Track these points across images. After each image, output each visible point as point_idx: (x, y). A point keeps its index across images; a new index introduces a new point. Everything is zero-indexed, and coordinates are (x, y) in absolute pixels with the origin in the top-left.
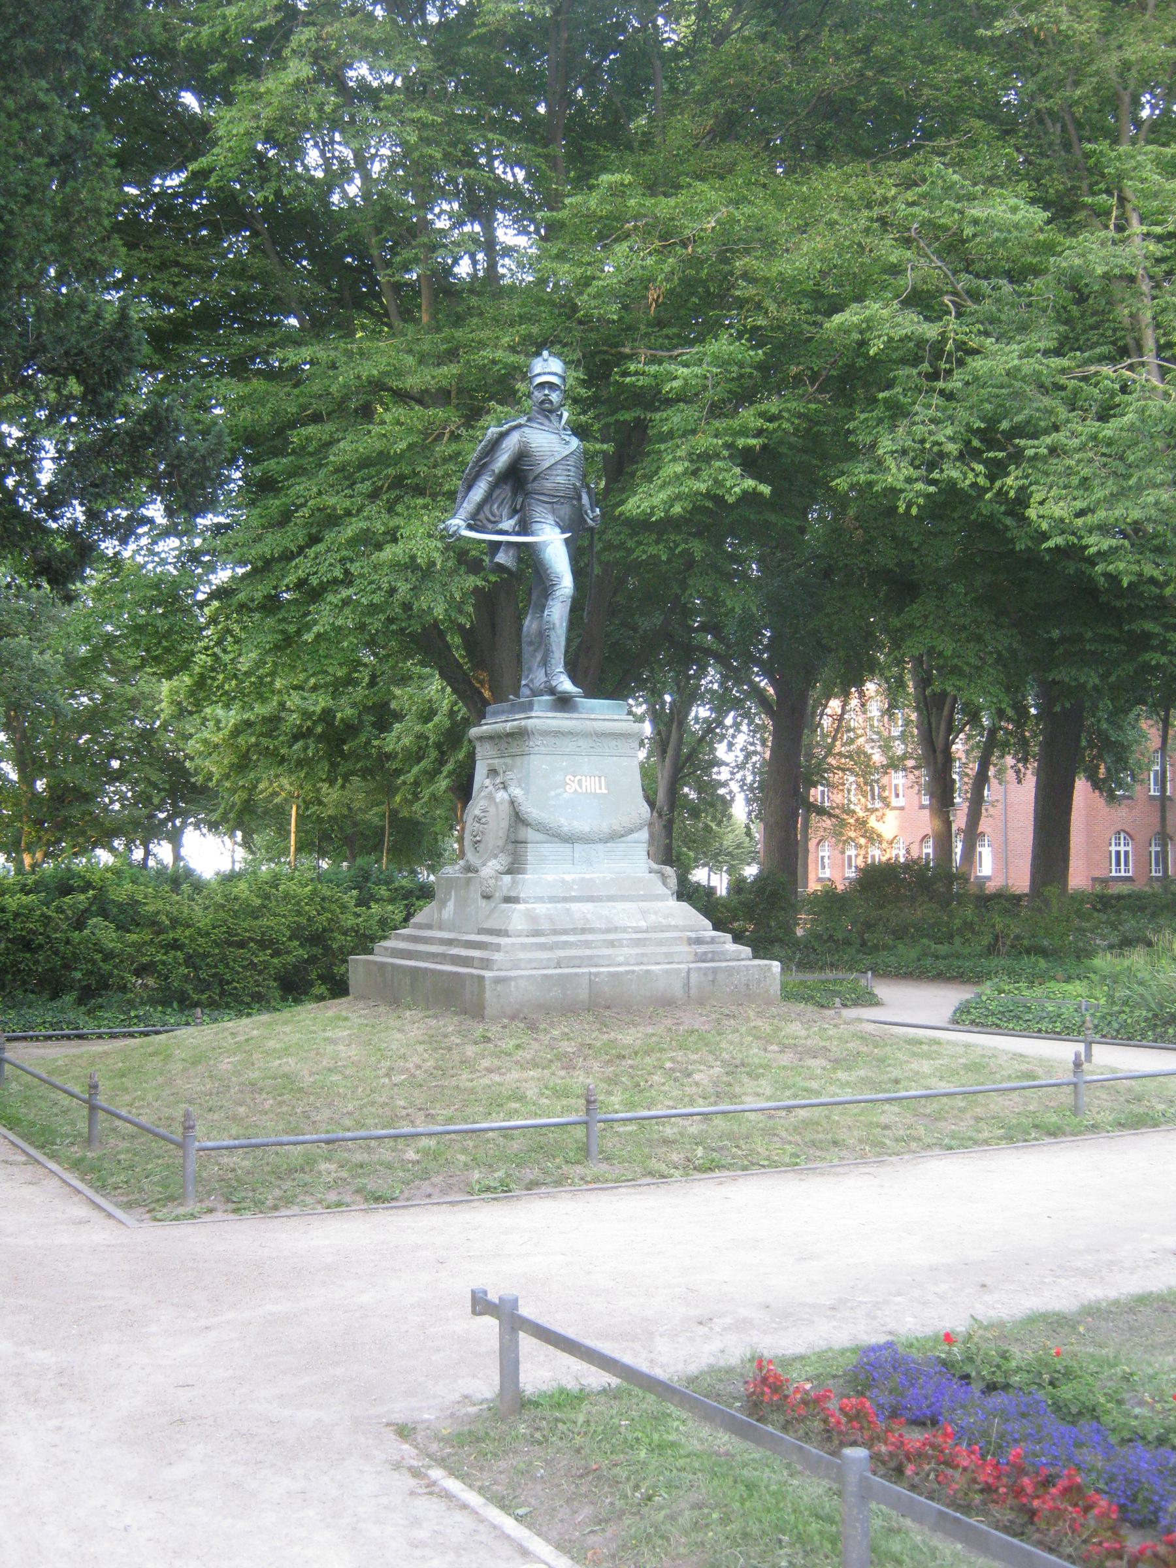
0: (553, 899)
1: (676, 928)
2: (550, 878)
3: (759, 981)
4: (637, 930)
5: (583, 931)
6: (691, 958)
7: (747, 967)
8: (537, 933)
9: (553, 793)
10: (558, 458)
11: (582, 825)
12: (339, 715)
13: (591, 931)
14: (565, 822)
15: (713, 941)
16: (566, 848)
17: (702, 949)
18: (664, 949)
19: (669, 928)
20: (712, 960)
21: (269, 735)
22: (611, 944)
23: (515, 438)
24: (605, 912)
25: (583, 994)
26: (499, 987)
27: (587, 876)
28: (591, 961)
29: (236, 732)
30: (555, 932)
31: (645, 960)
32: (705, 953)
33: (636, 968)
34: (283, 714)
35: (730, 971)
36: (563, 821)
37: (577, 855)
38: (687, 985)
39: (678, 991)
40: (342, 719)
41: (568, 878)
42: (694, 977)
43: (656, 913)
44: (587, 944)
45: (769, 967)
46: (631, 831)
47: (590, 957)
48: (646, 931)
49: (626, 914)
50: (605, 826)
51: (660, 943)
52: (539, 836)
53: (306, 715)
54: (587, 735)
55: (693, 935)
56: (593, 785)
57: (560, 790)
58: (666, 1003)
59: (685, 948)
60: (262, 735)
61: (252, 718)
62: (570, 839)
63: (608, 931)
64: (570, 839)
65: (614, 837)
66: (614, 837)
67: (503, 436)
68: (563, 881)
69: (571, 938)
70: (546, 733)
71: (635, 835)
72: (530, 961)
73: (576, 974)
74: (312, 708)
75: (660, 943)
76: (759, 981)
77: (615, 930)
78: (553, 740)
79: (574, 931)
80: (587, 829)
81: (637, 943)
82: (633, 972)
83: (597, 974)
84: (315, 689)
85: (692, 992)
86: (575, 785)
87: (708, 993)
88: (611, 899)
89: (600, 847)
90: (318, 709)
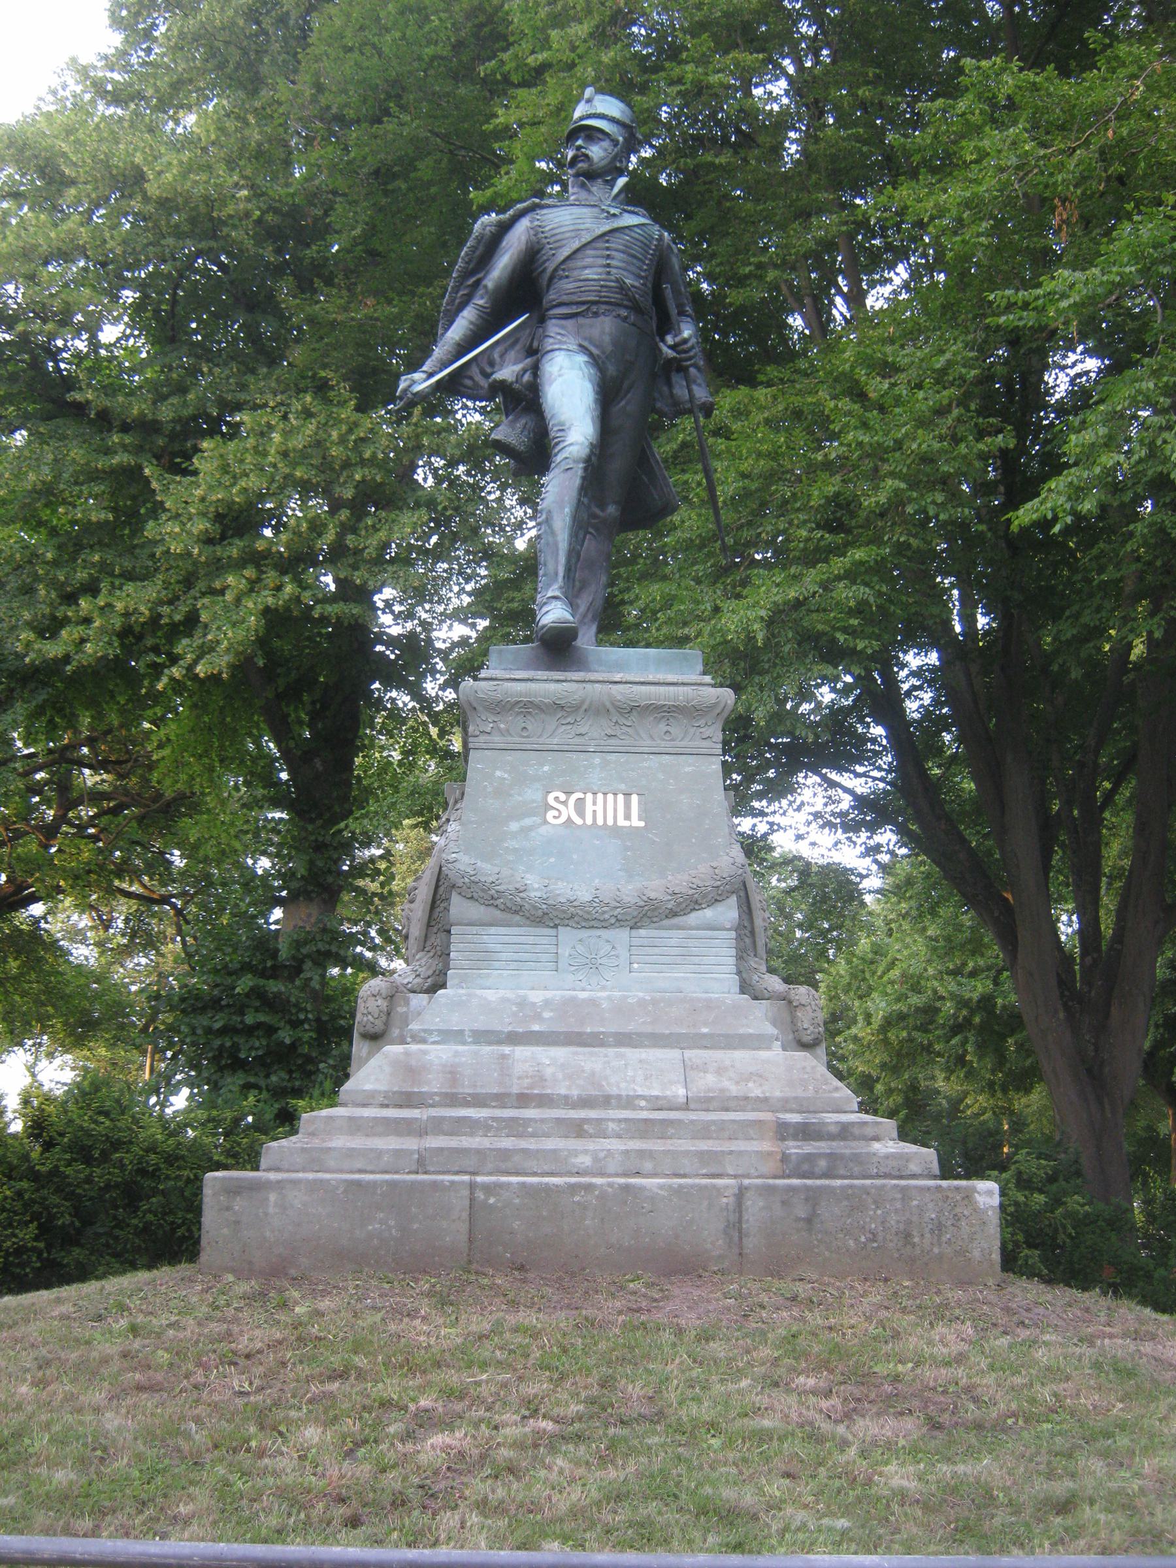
1: (763, 1103)
2: (491, 995)
3: (939, 1227)
4: (657, 1104)
5: (524, 1100)
6: (768, 1167)
7: (903, 1189)
8: (407, 1100)
9: (514, 826)
10: (587, 238)
11: (578, 890)
12: (999, 1001)
13: (544, 1101)
14: (534, 883)
15: (845, 1132)
16: (540, 937)
19: (744, 1102)
21: (923, 1028)
22: (578, 1129)
23: (524, 224)
25: (454, 1231)
26: (238, 1204)
28: (504, 1160)
29: (888, 1023)
30: (452, 1100)
31: (648, 1166)
32: (809, 1158)
34: (938, 1004)
35: (855, 1201)
37: (565, 951)
38: (735, 1227)
40: (1004, 1007)
41: (537, 997)
42: (754, 1207)
43: (720, 1071)
45: (968, 1196)
46: (693, 903)
47: (505, 1154)
48: (686, 1107)
50: (630, 891)
51: (704, 1131)
53: (963, 1003)
55: (794, 1118)
57: (528, 822)
58: (679, 1265)
59: (766, 1146)
60: (916, 1028)
61: (905, 1009)
62: (548, 917)
63: (585, 1102)
64: (548, 917)
65: (647, 915)
66: (647, 915)
67: (504, 228)
68: (522, 1003)
70: (500, 707)
71: (708, 914)
72: (351, 1153)
74: (967, 995)
75: (704, 1131)
76: (939, 1227)
77: (606, 1101)
78: (520, 722)
79: (501, 1099)
80: (584, 895)
81: (644, 1129)
82: (589, 1187)
83: (488, 1189)
84: (973, 974)
85: (750, 1243)
86: (569, 811)
87: (784, 1247)
88: (625, 1040)
89: (622, 936)
90: (975, 996)
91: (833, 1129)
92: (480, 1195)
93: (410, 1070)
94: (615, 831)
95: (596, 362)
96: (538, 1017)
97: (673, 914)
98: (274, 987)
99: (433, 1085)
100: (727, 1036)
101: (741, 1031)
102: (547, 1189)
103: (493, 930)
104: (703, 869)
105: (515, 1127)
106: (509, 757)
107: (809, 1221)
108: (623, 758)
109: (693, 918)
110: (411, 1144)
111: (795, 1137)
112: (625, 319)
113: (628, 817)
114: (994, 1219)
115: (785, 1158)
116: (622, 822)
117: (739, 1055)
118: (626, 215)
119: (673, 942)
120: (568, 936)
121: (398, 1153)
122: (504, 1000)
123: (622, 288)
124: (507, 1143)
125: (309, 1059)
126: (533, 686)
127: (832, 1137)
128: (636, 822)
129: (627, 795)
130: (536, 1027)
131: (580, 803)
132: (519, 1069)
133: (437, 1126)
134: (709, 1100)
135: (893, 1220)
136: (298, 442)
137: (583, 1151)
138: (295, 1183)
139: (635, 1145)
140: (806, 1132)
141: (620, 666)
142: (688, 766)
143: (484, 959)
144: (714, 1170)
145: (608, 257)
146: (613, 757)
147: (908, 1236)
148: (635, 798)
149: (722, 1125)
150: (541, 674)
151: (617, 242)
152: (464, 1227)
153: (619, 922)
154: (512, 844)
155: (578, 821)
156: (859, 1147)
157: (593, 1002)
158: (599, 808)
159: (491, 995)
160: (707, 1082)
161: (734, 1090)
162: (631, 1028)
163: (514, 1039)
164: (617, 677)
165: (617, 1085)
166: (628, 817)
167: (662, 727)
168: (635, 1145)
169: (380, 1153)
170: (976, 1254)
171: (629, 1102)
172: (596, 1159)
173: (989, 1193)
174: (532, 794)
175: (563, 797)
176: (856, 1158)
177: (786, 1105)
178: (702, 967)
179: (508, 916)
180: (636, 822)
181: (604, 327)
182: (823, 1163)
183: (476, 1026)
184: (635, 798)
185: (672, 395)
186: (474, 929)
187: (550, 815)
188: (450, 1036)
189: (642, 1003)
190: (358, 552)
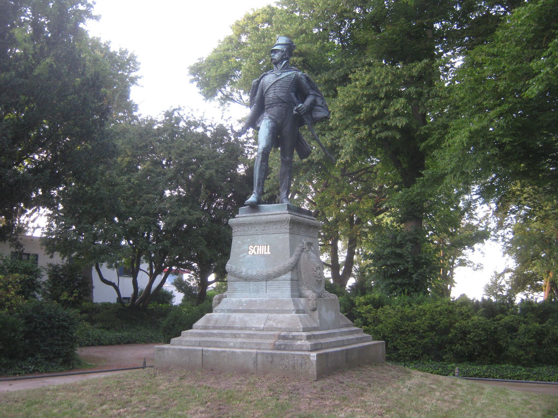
0: (230, 311)
3: (301, 365)
5: (229, 328)
7: (293, 355)
8: (205, 328)
9: (241, 256)
13: (233, 328)
14: (244, 270)
17: (281, 342)
18: (255, 341)
20: (284, 349)
22: (235, 336)
24: (247, 318)
25: (199, 361)
26: (160, 353)
27: (254, 299)
28: (216, 344)
30: (214, 328)
31: (245, 346)
32: (280, 345)
33: (238, 350)
35: (282, 357)
36: (244, 270)
38: (256, 363)
39: (251, 366)
41: (243, 300)
42: (260, 357)
44: (222, 335)
45: (308, 357)
48: (263, 330)
49: (257, 321)
51: (262, 337)
52: (232, 278)
55: (283, 333)
56: (263, 250)
57: (244, 254)
58: (243, 371)
62: (247, 279)
63: (241, 329)
64: (247, 279)
65: (268, 278)
66: (268, 278)
68: (240, 302)
69: (215, 331)
70: (239, 225)
71: (284, 276)
72: (187, 341)
73: (195, 350)
76: (301, 365)
77: (246, 328)
78: (243, 228)
79: (224, 328)
80: (254, 273)
81: (249, 336)
82: (225, 352)
83: (206, 351)
85: (259, 367)
86: (254, 251)
88: (259, 311)
89: (264, 283)
91: (291, 337)
92: (204, 353)
93: (209, 320)
94: (264, 255)
95: (273, 120)
96: (242, 305)
97: (276, 277)
98: (398, 251)
99: (211, 324)
100: (282, 310)
101: (286, 309)
102: (216, 352)
103: (236, 283)
104: (282, 265)
105: (222, 335)
106: (241, 237)
107: (272, 362)
108: (266, 235)
109: (281, 278)
110: (198, 339)
111: (282, 339)
112: (281, 106)
113: (267, 251)
114: (314, 363)
115: (274, 345)
116: (265, 253)
117: (281, 315)
118: (283, 74)
119: (276, 284)
120: (252, 284)
121: (195, 341)
122: (237, 301)
123: (279, 98)
126: (245, 219)
127: (290, 339)
128: (269, 253)
129: (267, 245)
130: (240, 308)
131: (256, 248)
132: (232, 319)
134: (267, 328)
135: (291, 362)
137: (231, 341)
138: (170, 349)
139: (245, 340)
140: (285, 338)
141: (268, 210)
142: (281, 236)
143: (235, 290)
144: (258, 347)
145: (275, 90)
146: (264, 235)
147: (294, 366)
148: (268, 246)
149: (266, 335)
150: (249, 215)
151: (278, 85)
152: (201, 360)
153: (262, 280)
154: (241, 260)
155: (255, 253)
157: (256, 301)
158: (260, 250)
159: (234, 299)
160: (271, 323)
161: (275, 325)
162: (261, 308)
163: (235, 311)
164: (266, 213)
165: (249, 325)
166: (267, 251)
167: (275, 226)
168: (245, 340)
169: (192, 341)
170: (310, 372)
171: (250, 329)
172: (234, 344)
173: (314, 356)
174: (245, 247)
175: (252, 247)
176: (291, 345)
177: (285, 330)
178: (282, 291)
179: (238, 279)
180: (269, 253)
181: (275, 110)
182: (283, 346)
183: (228, 308)
184: (268, 246)
185: (312, 117)
186: (233, 283)
187: (250, 252)
188: (222, 311)
189: (266, 301)
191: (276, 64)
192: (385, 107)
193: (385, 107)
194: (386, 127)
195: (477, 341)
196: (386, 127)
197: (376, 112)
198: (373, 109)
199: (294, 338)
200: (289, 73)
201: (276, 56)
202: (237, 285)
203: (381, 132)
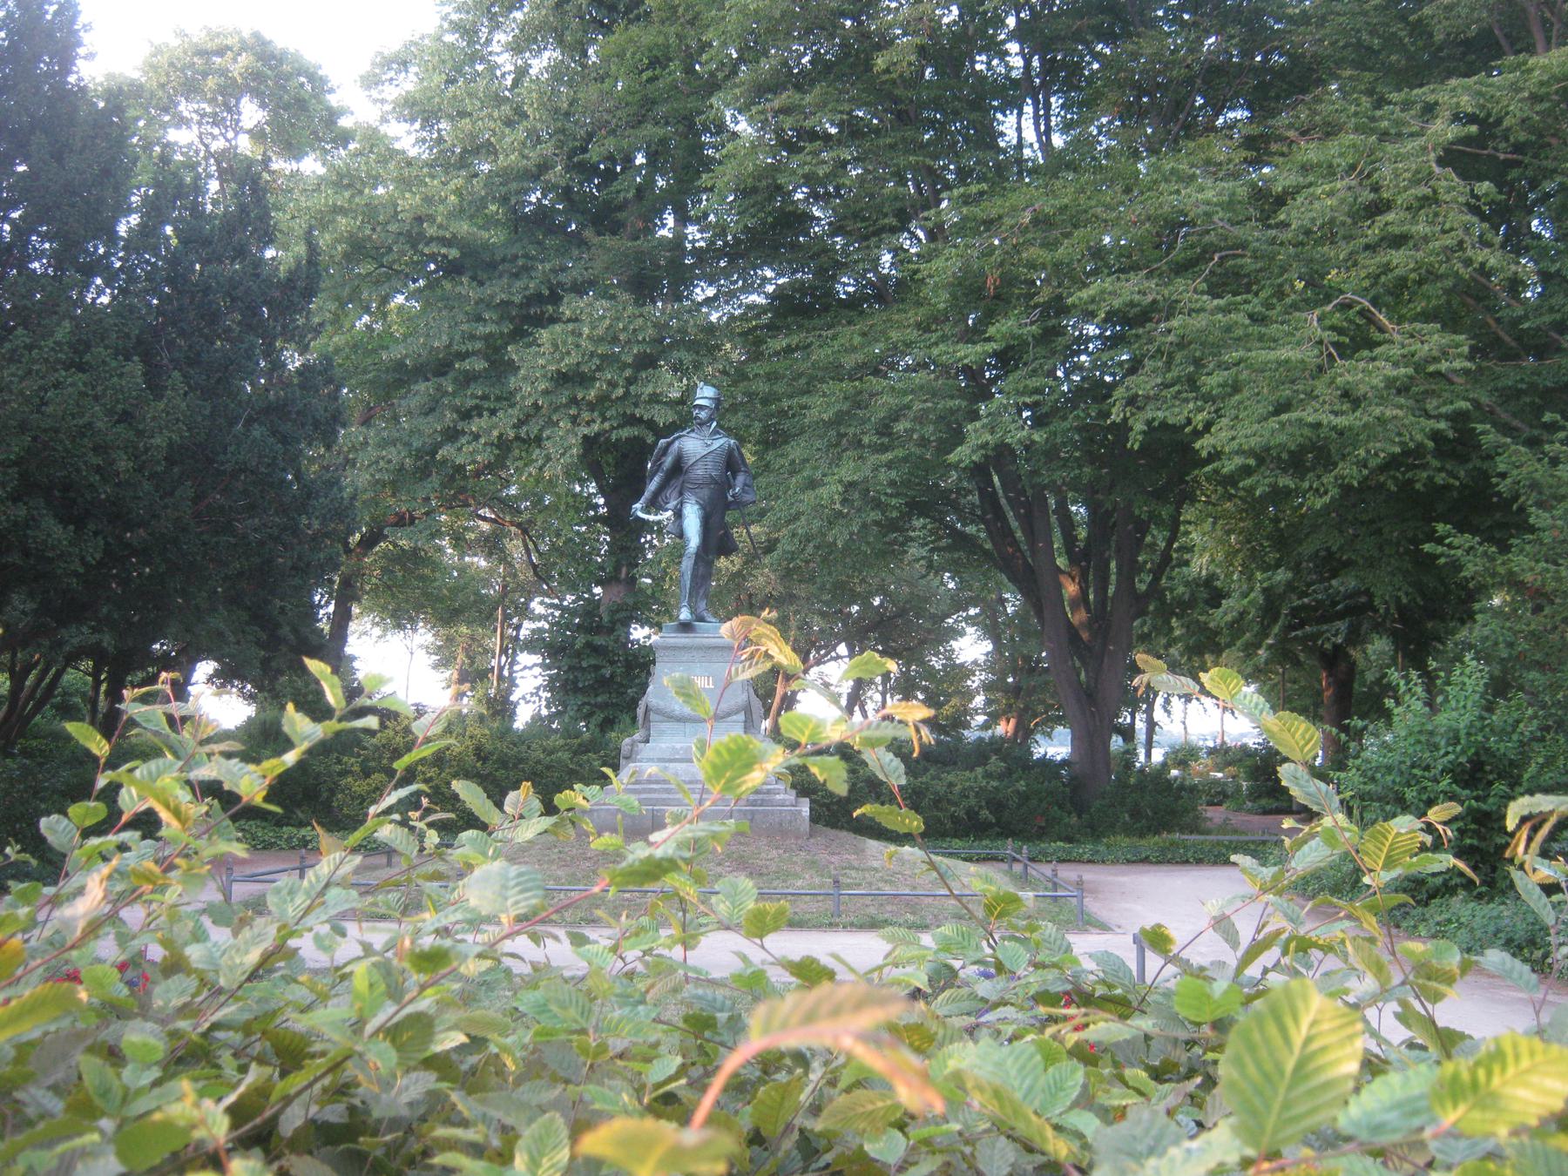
8: (637, 782)
35: (765, 813)
41: (678, 746)
46: (729, 715)
52: (658, 717)
54: (699, 648)
95: (703, 507)
98: (599, 640)
124: (665, 796)
125: (622, 685)
133: (644, 791)
136: (600, 331)
143: (662, 733)
156: (771, 797)
163: (671, 761)
181: (706, 493)
190: (638, 396)
191: (701, 424)
192: (630, 381)
193: (630, 381)
194: (633, 420)
195: (824, 805)
196: (633, 420)
197: (620, 391)
198: (612, 384)
199: (768, 792)
200: (722, 441)
201: (703, 415)
202: (665, 726)
203: (620, 426)
